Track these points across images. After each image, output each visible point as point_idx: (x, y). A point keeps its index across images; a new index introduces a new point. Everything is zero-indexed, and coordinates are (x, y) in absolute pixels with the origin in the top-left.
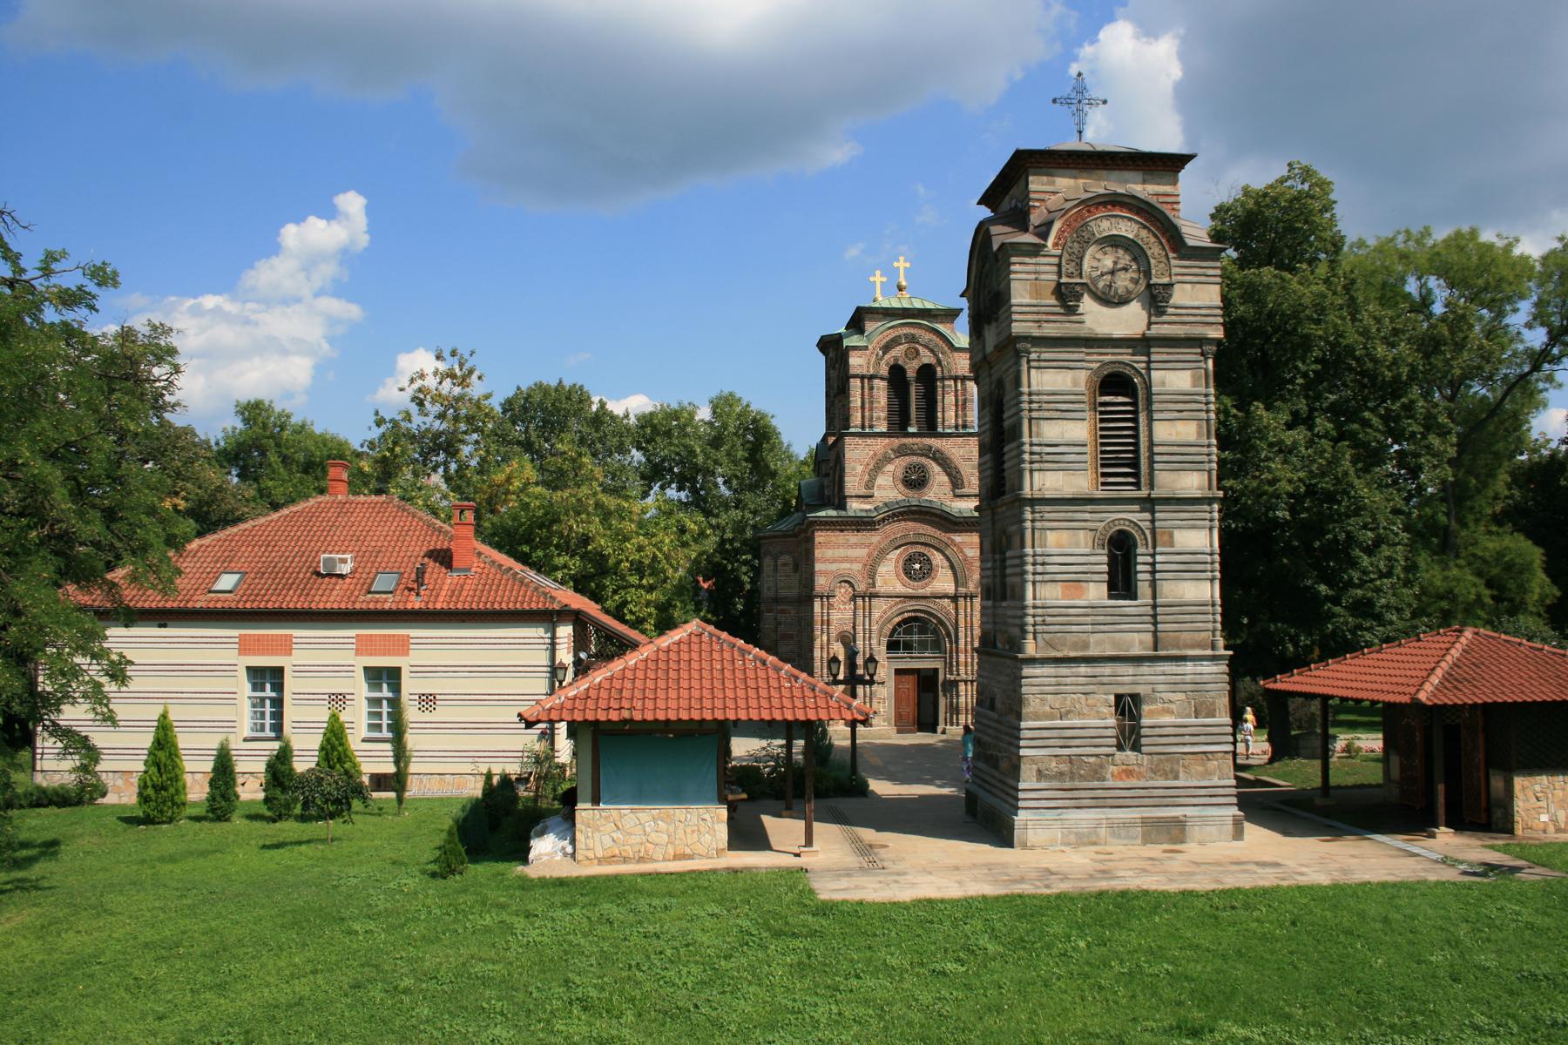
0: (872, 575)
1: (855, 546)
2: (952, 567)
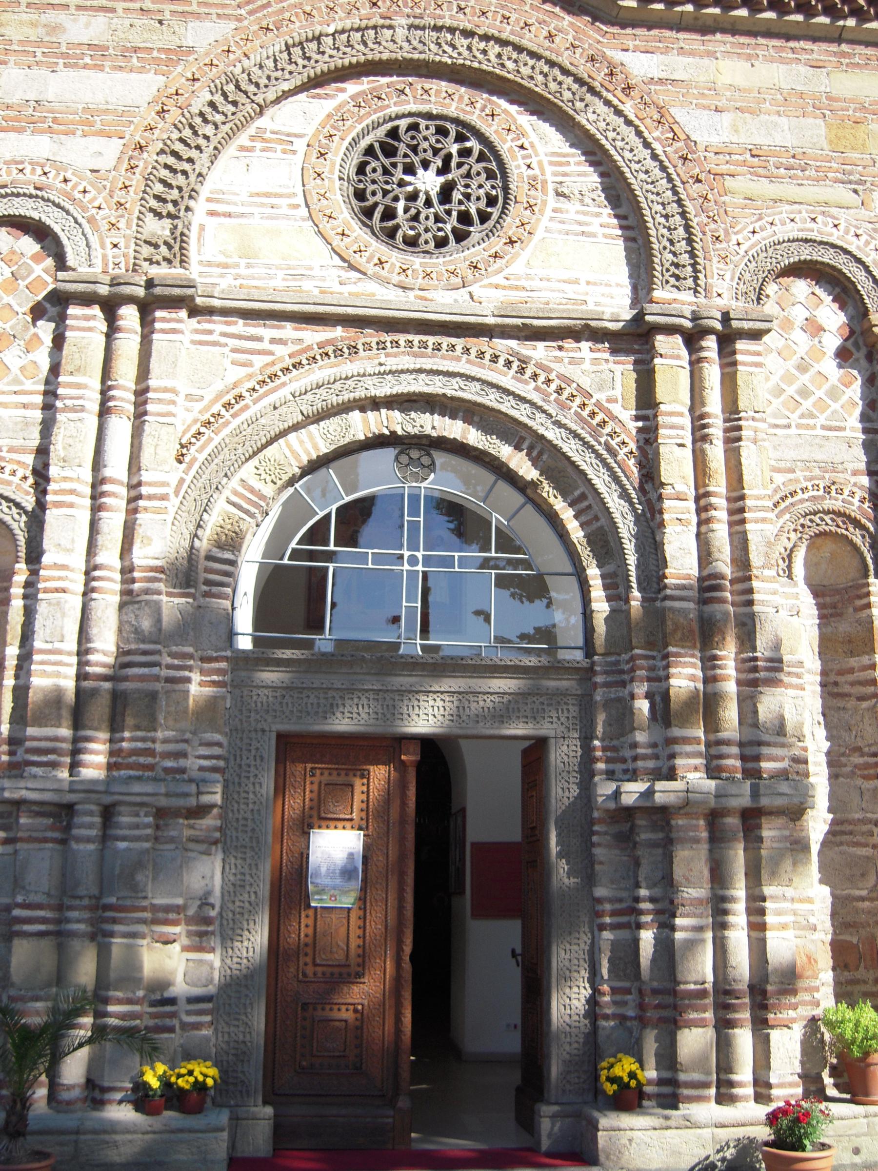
0: (171, 196)
1: (97, 55)
2: (618, 193)
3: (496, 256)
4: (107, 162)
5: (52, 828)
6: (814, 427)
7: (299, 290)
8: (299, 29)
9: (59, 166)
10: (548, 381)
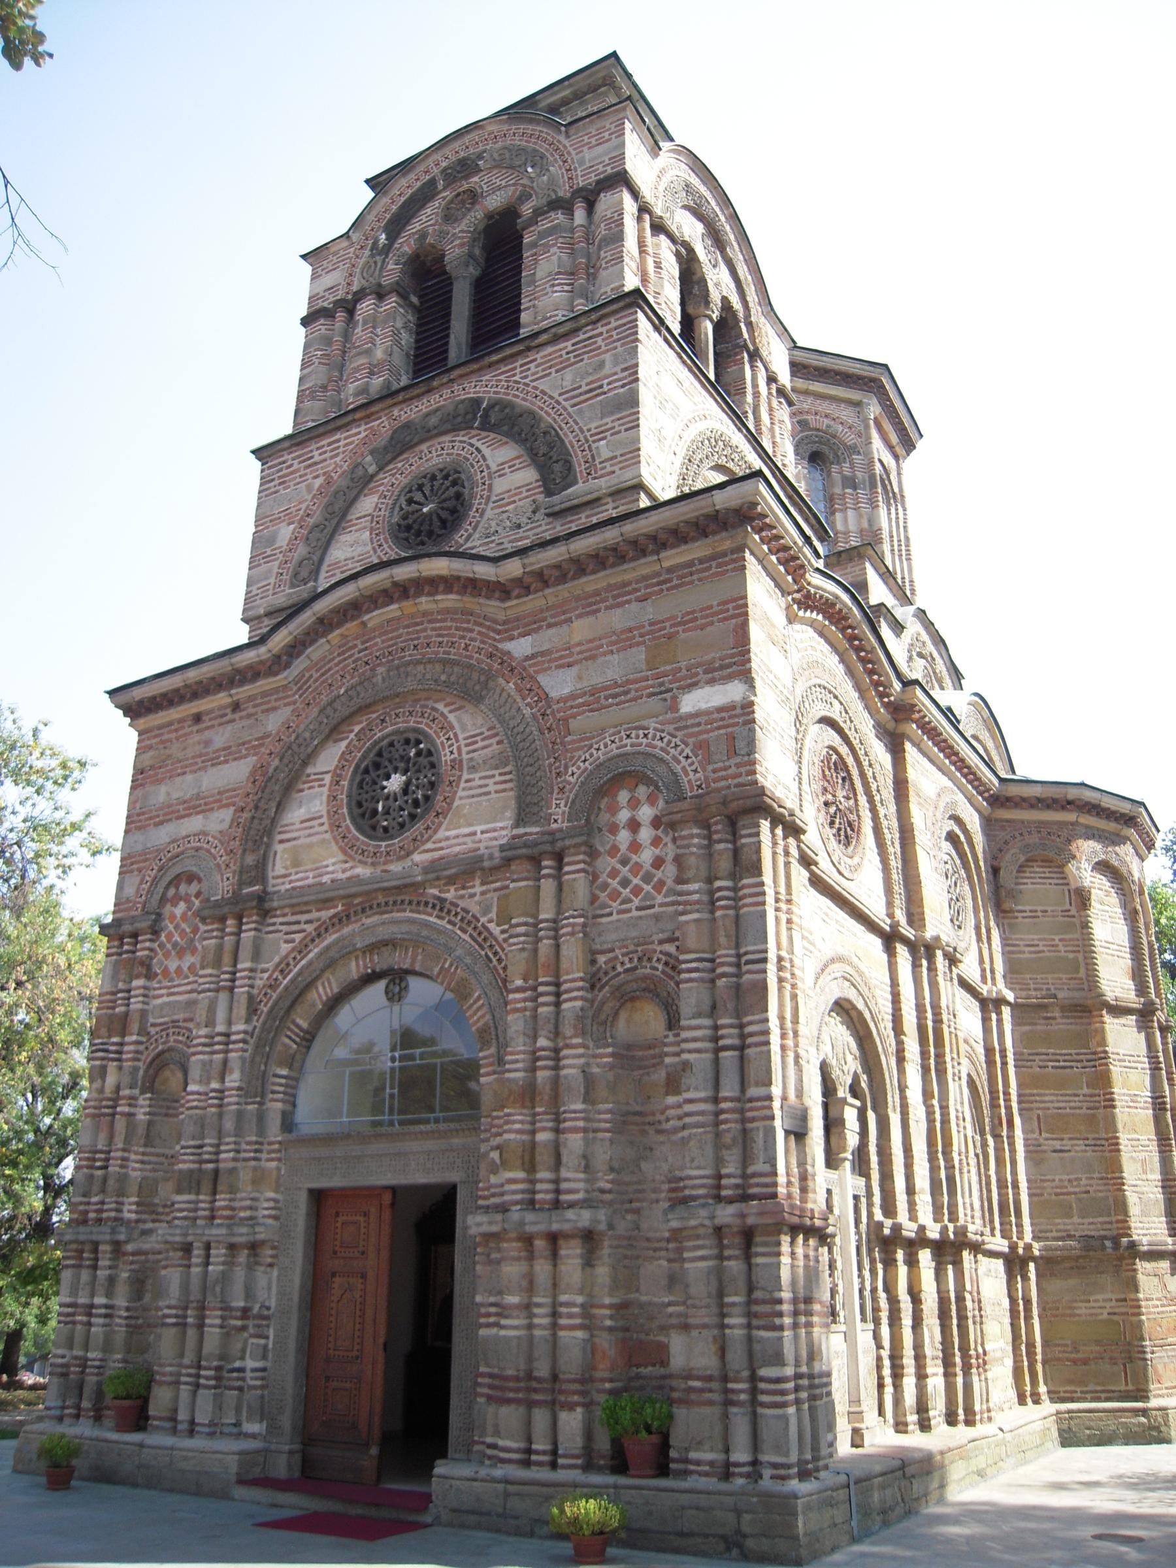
3: (428, 828)
4: (226, 825)
5: (182, 1258)
6: (629, 911)
7: (321, 884)
8: (324, 699)
9: (205, 834)
10: (456, 914)
